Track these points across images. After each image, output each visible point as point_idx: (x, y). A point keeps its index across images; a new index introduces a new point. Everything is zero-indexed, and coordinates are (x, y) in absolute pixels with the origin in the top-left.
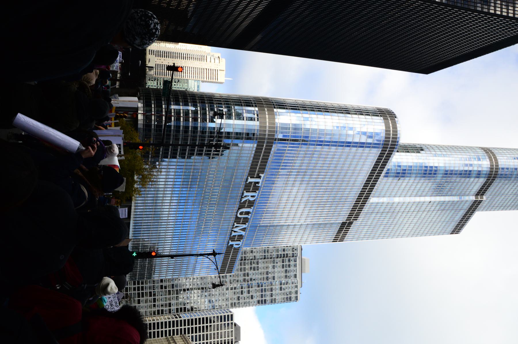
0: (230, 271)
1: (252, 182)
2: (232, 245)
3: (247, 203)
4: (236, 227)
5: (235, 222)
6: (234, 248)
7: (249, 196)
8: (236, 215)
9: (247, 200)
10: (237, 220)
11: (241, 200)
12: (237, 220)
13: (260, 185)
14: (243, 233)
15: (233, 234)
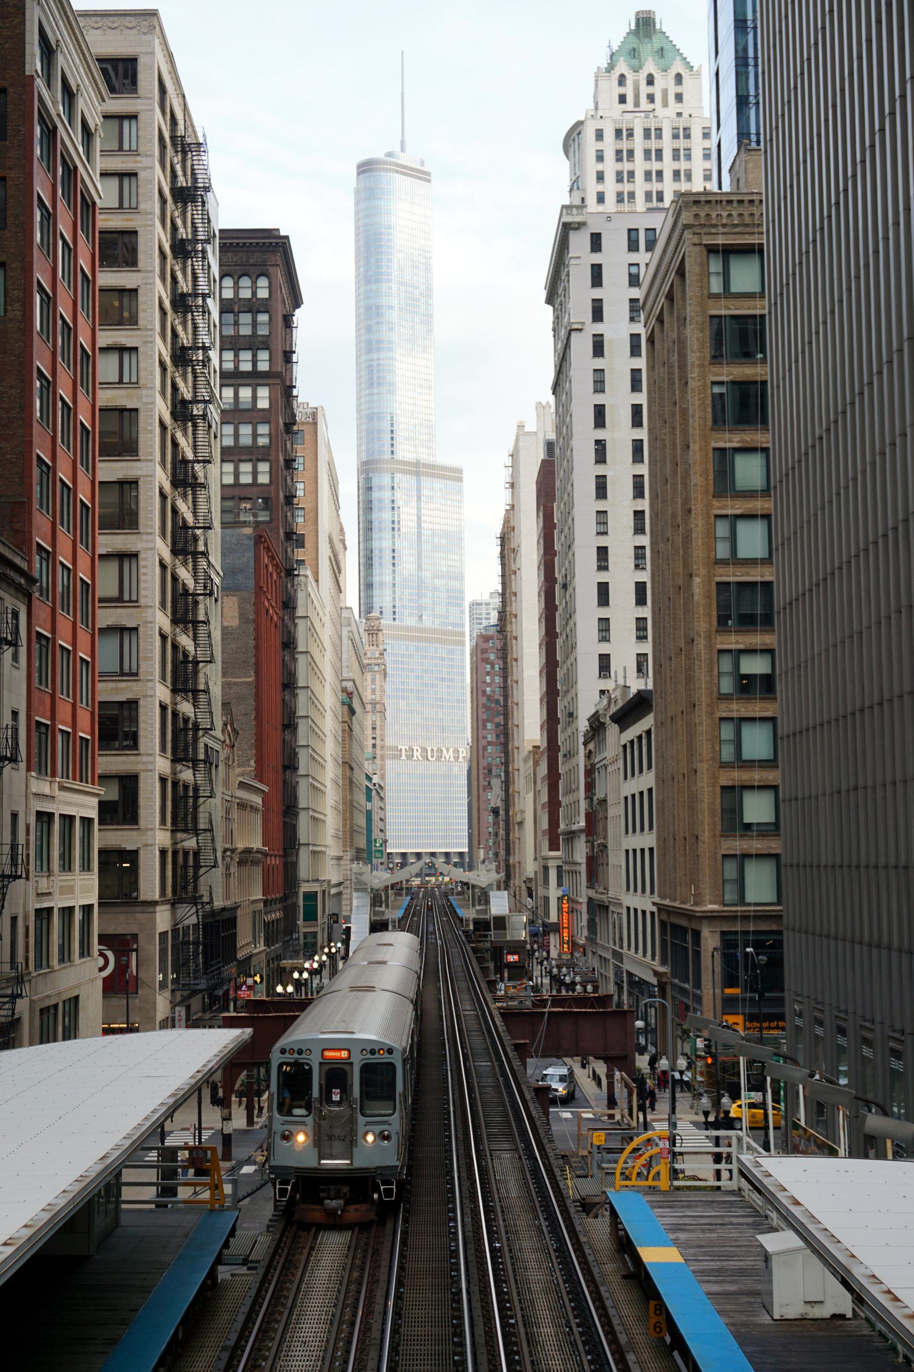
12: (439, 758)
14: (451, 750)
15: (452, 759)
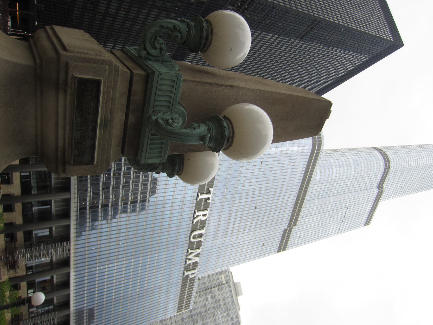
0: (188, 306)
1: (202, 199)
2: (188, 276)
3: (199, 224)
4: (191, 253)
5: (188, 248)
6: (191, 278)
7: (200, 215)
8: (190, 240)
9: (198, 222)
10: (191, 246)
11: (193, 221)
12: (191, 246)
13: (210, 201)
14: (197, 259)
15: (188, 262)
